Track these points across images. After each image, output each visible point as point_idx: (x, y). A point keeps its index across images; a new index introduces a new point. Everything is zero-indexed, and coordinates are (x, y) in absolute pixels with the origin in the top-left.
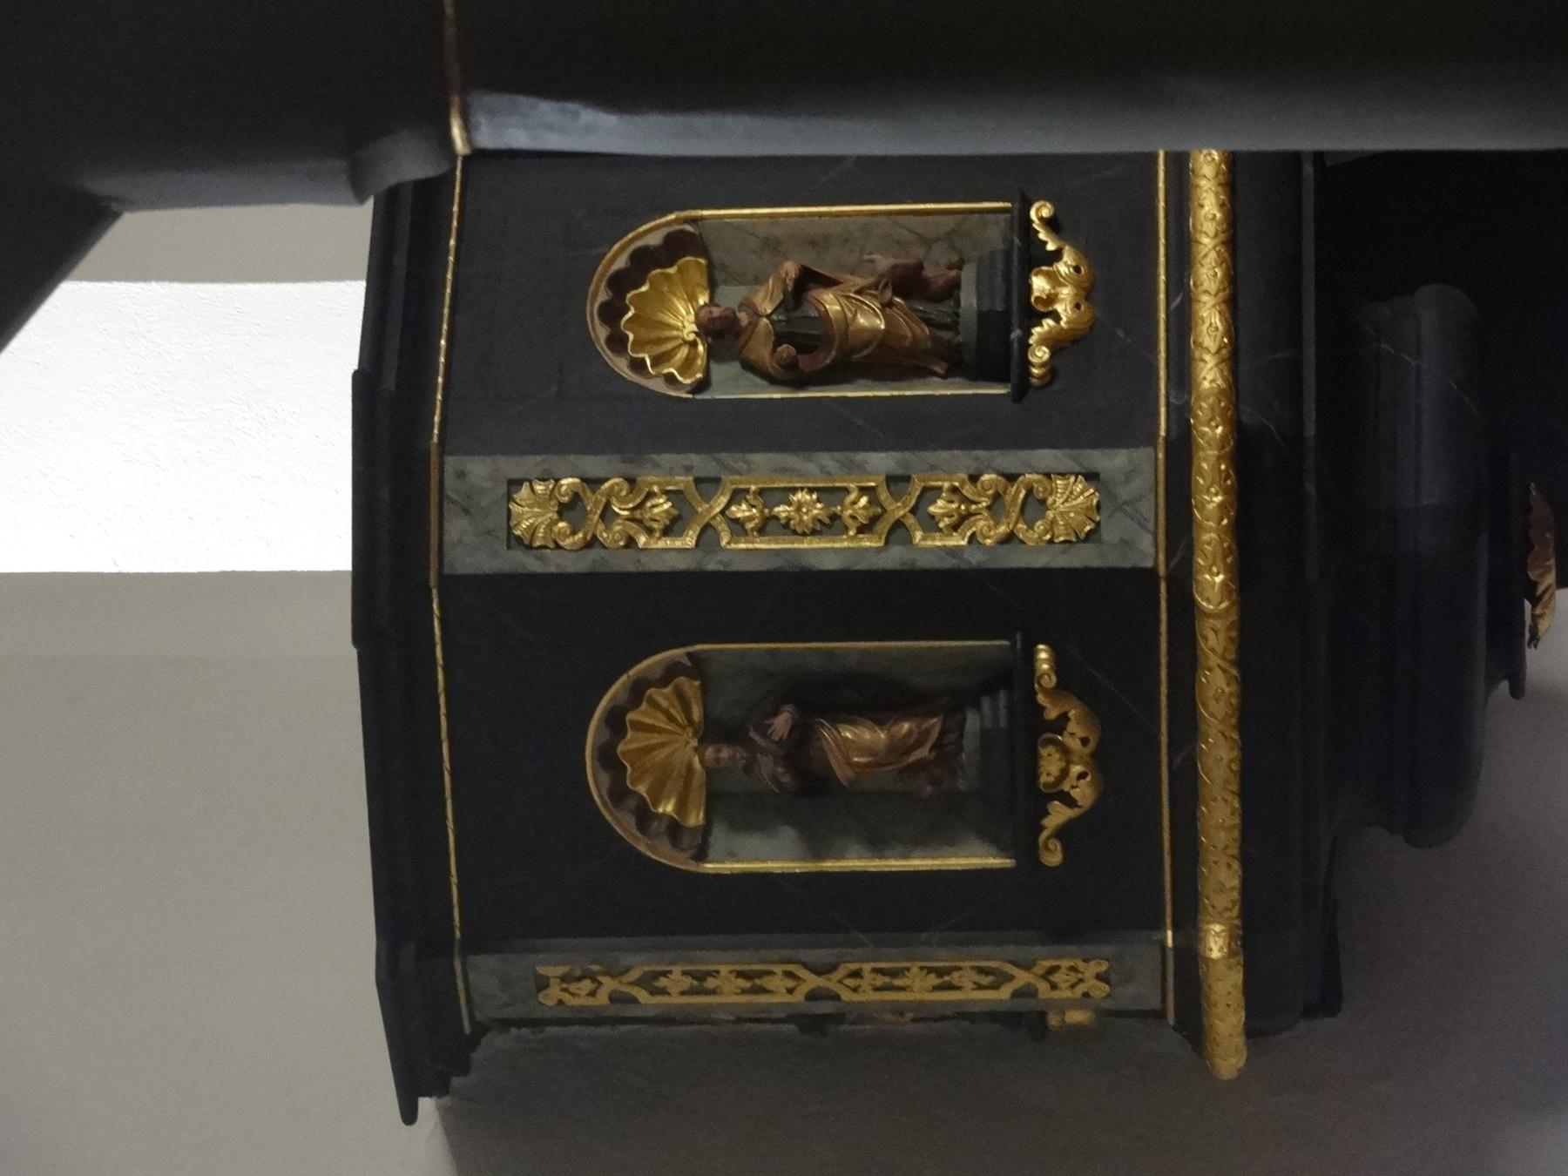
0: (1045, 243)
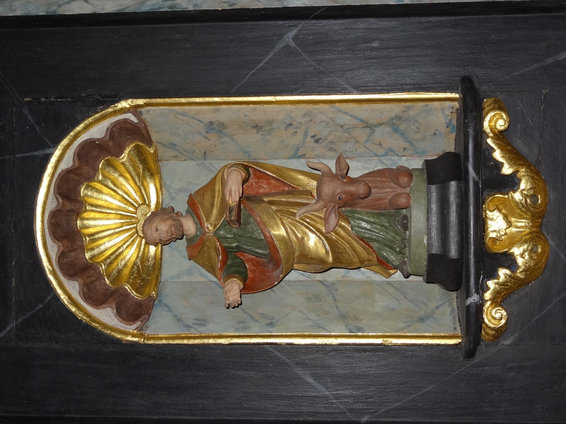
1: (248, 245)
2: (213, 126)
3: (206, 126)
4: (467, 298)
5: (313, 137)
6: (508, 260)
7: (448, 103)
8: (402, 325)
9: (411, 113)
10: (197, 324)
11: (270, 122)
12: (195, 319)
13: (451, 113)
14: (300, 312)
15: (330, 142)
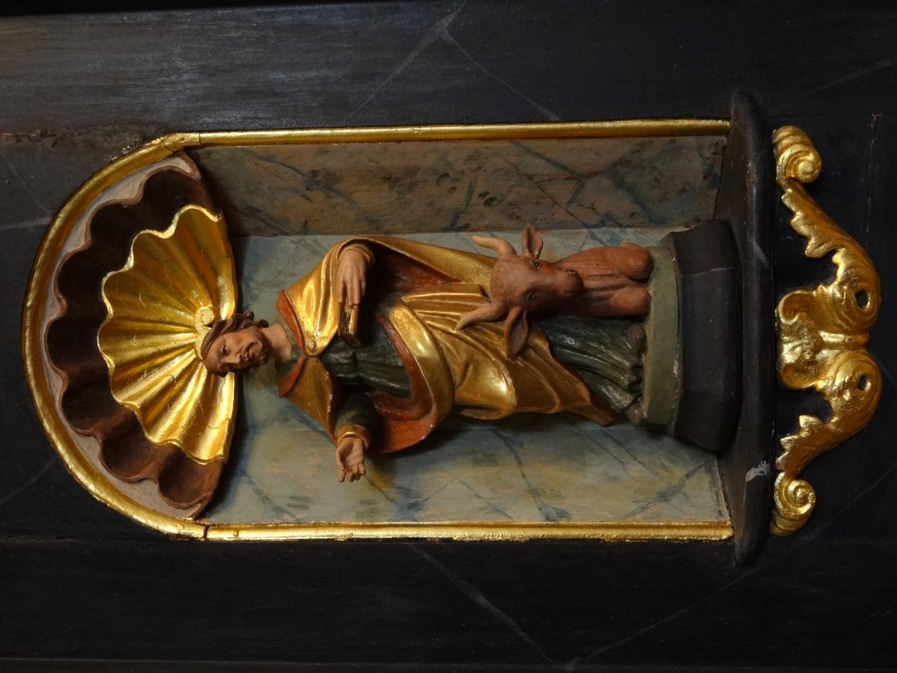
0: (805, 239)
1: (376, 376)
2: (318, 179)
3: (306, 179)
4: (749, 468)
5: (482, 195)
6: (816, 403)
7: (708, 140)
8: (633, 507)
9: (647, 154)
10: (293, 506)
11: (413, 171)
12: (291, 497)
13: (714, 153)
14: (464, 484)
15: (511, 204)
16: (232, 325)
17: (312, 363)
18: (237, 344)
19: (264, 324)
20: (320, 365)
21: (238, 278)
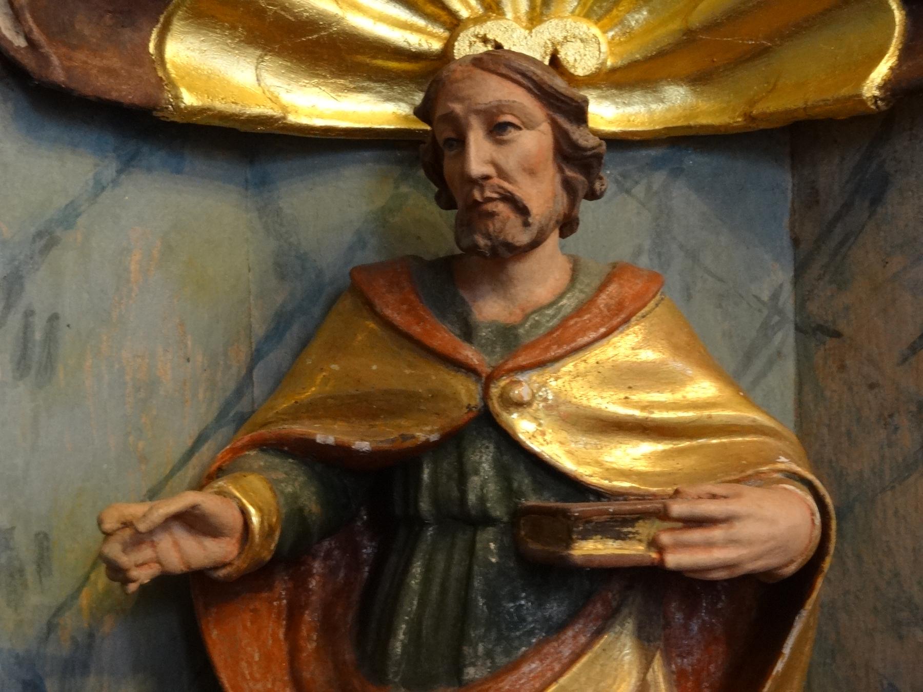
1: (427, 580)
10: (27, 328)
12: (54, 318)
16: (575, 146)
17: (466, 392)
18: (516, 161)
19: (567, 225)
20: (459, 416)
21: (677, 142)
